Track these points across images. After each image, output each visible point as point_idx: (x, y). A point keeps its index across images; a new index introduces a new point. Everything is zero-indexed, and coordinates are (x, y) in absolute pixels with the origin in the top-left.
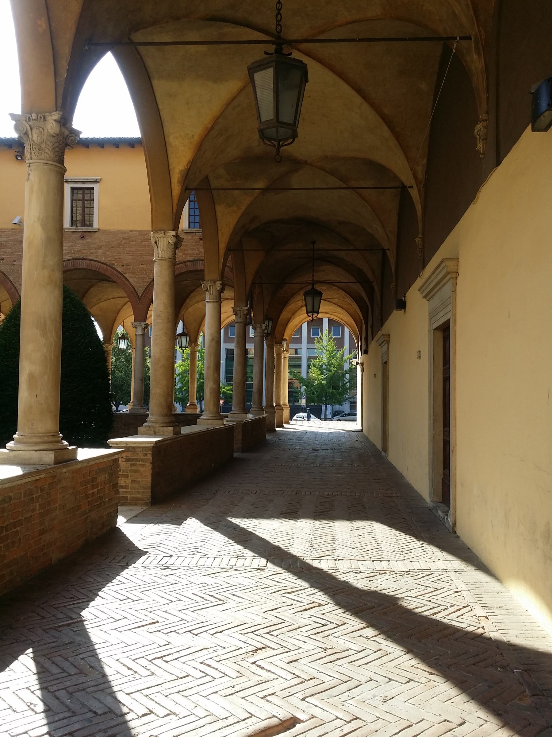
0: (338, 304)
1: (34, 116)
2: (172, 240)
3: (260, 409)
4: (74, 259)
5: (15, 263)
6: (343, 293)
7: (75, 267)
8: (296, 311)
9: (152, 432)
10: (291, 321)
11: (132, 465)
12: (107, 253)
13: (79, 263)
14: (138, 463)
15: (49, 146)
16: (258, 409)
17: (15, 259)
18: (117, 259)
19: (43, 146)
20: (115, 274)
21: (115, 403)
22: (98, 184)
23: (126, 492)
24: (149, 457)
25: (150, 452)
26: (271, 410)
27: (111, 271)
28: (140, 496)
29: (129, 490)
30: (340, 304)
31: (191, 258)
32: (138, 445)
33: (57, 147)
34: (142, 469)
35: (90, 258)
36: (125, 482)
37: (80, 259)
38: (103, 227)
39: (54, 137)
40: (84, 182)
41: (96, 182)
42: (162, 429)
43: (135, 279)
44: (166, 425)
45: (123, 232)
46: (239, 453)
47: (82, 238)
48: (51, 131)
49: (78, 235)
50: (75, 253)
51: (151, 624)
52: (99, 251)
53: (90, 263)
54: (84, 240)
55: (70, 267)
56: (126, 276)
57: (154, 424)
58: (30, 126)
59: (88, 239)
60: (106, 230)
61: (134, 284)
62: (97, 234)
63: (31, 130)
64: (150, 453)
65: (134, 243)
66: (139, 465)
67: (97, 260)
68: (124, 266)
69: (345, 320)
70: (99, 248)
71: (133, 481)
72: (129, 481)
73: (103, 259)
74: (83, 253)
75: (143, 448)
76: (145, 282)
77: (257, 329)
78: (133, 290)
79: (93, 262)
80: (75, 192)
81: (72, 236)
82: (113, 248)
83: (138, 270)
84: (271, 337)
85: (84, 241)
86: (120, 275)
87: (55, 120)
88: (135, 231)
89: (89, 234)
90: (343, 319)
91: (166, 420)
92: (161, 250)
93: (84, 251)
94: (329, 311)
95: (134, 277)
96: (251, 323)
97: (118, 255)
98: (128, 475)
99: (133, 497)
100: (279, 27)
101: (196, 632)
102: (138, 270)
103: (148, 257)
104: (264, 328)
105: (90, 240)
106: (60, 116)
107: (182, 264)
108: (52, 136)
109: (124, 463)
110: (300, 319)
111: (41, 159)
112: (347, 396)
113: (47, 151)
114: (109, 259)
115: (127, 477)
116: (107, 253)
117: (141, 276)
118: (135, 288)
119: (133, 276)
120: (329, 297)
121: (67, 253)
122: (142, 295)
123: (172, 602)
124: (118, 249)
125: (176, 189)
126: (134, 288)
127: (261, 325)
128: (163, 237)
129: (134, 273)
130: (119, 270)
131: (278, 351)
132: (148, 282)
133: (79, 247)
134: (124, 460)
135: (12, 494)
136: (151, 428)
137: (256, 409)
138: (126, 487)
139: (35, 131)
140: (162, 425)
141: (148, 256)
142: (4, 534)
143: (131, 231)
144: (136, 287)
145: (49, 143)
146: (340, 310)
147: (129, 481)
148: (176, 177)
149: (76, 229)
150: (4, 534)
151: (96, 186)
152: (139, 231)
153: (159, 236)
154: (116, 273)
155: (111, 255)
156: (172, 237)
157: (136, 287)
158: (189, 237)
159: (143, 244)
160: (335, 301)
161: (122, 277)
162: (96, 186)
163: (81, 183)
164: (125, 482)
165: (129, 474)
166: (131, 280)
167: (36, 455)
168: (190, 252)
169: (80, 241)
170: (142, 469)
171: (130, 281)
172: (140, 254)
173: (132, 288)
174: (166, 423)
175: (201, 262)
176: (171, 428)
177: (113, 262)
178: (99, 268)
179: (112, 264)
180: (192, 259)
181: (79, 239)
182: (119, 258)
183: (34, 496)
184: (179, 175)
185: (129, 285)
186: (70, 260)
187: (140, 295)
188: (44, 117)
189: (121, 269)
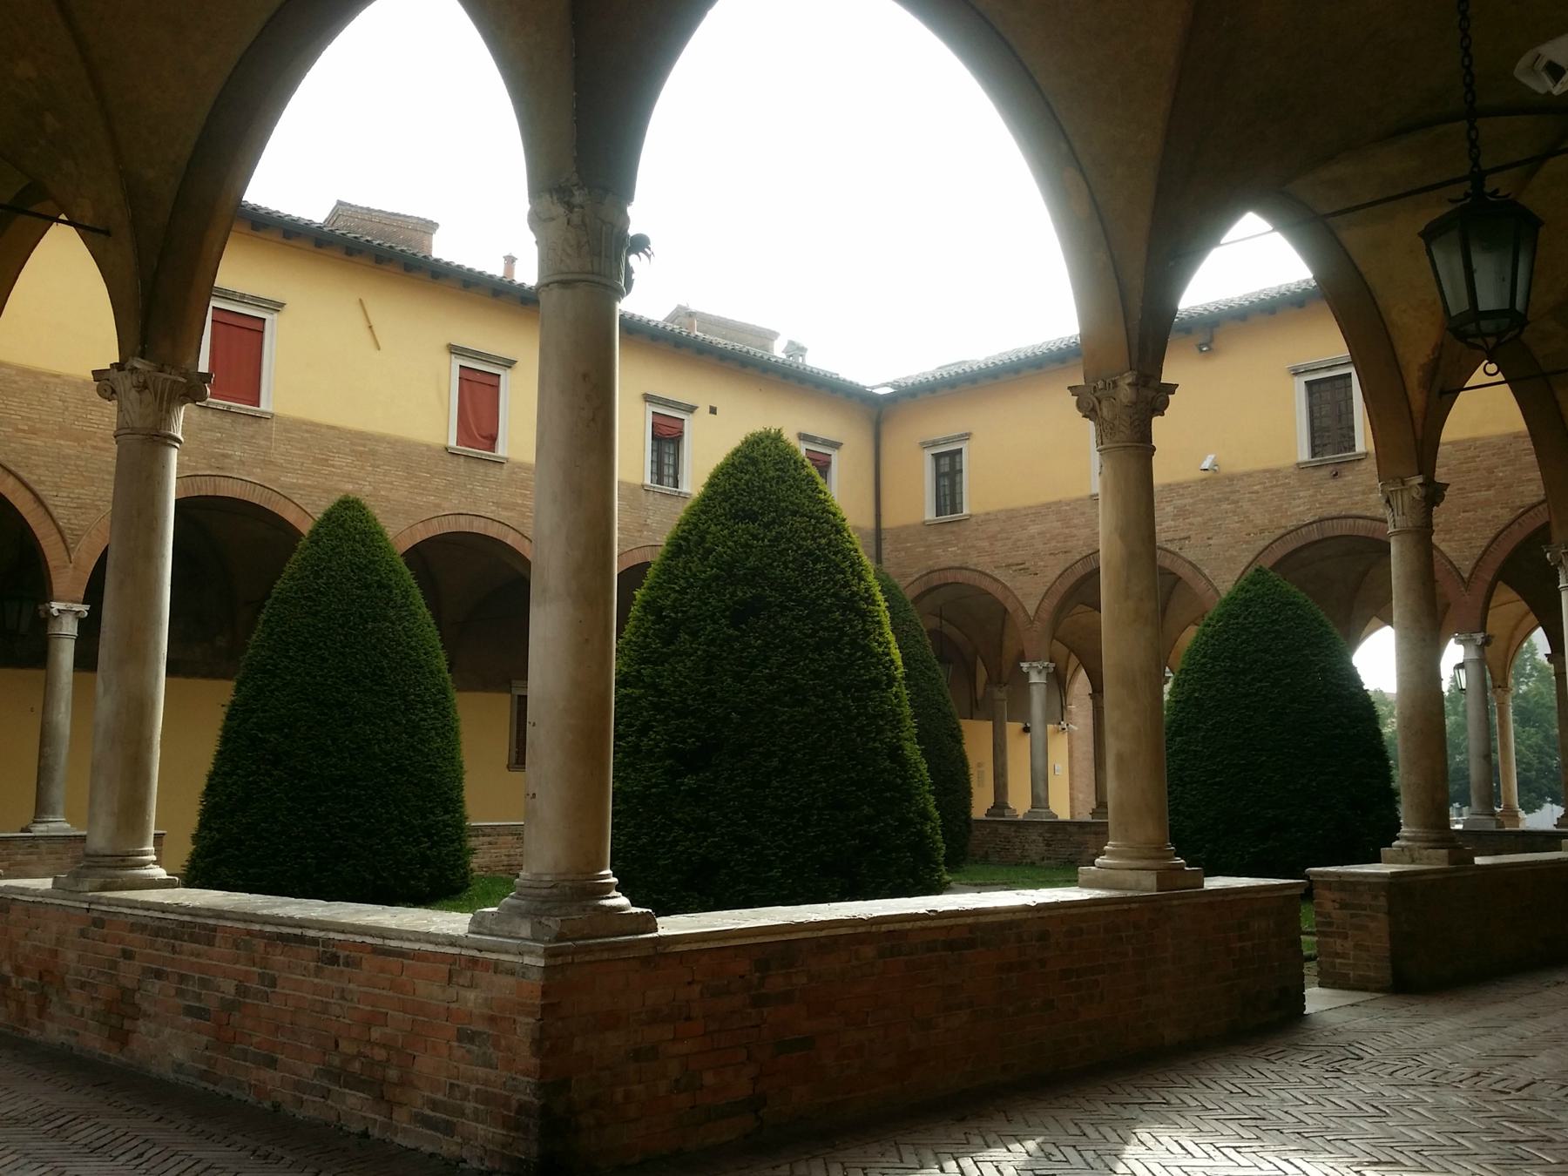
1: (1100, 384)
2: (1417, 493)
4: (1321, 520)
5: (1211, 542)
7: (1325, 536)
9: (1407, 858)
11: (1352, 916)
13: (1333, 526)
14: (1363, 912)
15: (1124, 420)
17: (1210, 535)
19: (1117, 422)
23: (1346, 964)
24: (1382, 901)
25: (1383, 893)
28: (1372, 974)
29: (1351, 962)
32: (1361, 879)
33: (1137, 419)
34: (1372, 925)
35: (1354, 512)
36: (1342, 946)
37: (1332, 519)
39: (1131, 407)
40: (1329, 368)
42: (1425, 853)
43: (1453, 544)
44: (1431, 845)
47: (1335, 475)
48: (1125, 401)
49: (1325, 472)
50: (1321, 508)
51: (1250, 1119)
52: (1371, 496)
55: (1316, 536)
57: (1410, 843)
58: (1097, 398)
59: (1345, 476)
61: (1452, 555)
63: (1100, 403)
64: (1384, 896)
66: (1367, 916)
67: (1368, 514)
71: (1357, 946)
72: (1349, 944)
74: (1340, 505)
75: (1369, 883)
76: (1475, 547)
78: (1449, 567)
79: (1361, 521)
80: (1315, 388)
81: (1316, 474)
83: (1458, 523)
85: (1339, 482)
87: (1129, 384)
89: (1349, 466)
91: (1433, 836)
92: (1400, 513)
95: (1449, 541)
98: (1347, 934)
99: (1360, 975)
100: (1475, 150)
101: (1306, 1135)
102: (1458, 523)
103: (1477, 494)
105: (1351, 478)
106: (1135, 377)
108: (1127, 406)
109: (1338, 911)
111: (1118, 442)
113: (1122, 428)
115: (1346, 937)
117: (1466, 535)
118: (1455, 563)
119: (1448, 537)
121: (1308, 509)
122: (1471, 575)
123: (1307, 1104)
125: (1417, 398)
126: (1451, 563)
128: (1401, 490)
129: (1449, 531)
132: (1481, 546)
133: (1330, 494)
134: (1337, 906)
135: (1084, 925)
136: (1405, 849)
138: (1343, 956)
139: (1104, 403)
140: (1426, 844)
141: (1477, 491)
142: (1074, 980)
145: (1124, 417)
147: (1349, 944)
148: (1414, 377)
149: (1321, 461)
150: (1074, 980)
153: (1393, 489)
156: (1418, 487)
164: (1342, 946)
165: (1350, 932)
167: (1131, 877)
169: (1332, 483)
170: (1372, 925)
171: (1442, 548)
172: (1459, 489)
173: (1447, 564)
174: (1434, 841)
176: (1444, 852)
181: (1326, 479)
183: (1124, 935)
184: (1421, 374)
186: (1314, 522)
188: (1114, 382)
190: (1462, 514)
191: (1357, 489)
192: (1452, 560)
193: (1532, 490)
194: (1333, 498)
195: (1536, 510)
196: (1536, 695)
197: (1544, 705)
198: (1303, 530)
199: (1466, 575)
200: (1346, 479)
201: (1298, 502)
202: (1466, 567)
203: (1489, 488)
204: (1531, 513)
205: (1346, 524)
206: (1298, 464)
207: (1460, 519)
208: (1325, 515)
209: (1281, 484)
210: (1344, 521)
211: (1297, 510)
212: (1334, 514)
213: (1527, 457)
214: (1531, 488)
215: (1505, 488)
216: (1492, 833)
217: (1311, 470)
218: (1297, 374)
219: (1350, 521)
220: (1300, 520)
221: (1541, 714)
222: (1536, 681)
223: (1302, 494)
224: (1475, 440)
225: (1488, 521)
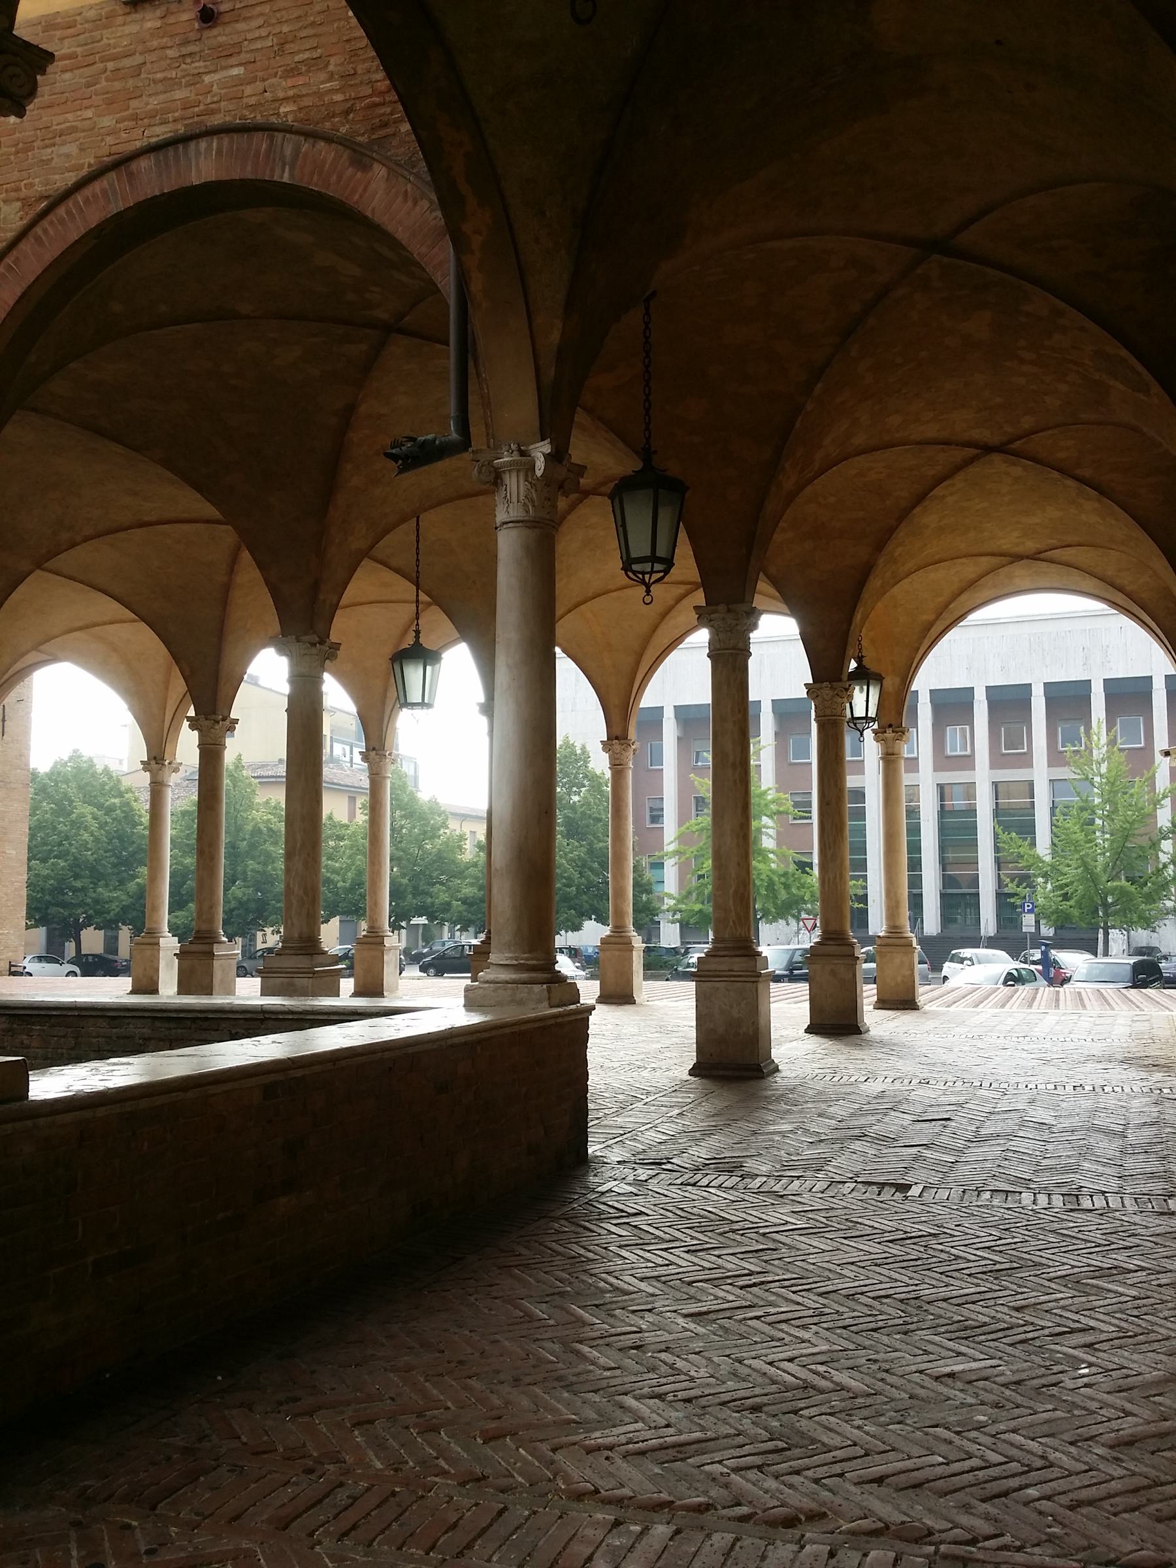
0: (1078, 472)
3: (524, 976)
8: (891, 531)
10: (874, 583)
16: (514, 976)
30: (1086, 472)
31: (159, 130)
69: (1129, 588)
84: (729, 611)
90: (1118, 582)
94: (1054, 542)
96: (465, 443)
107: (113, 175)
110: (940, 599)
120: (1027, 422)
127: (523, 453)
131: (828, 712)
137: (504, 975)
158: (149, 25)
168: (154, 102)
175: (203, 144)
180: (161, 132)
193: (68, 156)
195: (70, 203)
196: (583, 805)
197: (590, 816)
204: (61, 211)
213: (67, 76)
214: (65, 149)
215: (17, 152)
221: (588, 826)
222: (588, 791)
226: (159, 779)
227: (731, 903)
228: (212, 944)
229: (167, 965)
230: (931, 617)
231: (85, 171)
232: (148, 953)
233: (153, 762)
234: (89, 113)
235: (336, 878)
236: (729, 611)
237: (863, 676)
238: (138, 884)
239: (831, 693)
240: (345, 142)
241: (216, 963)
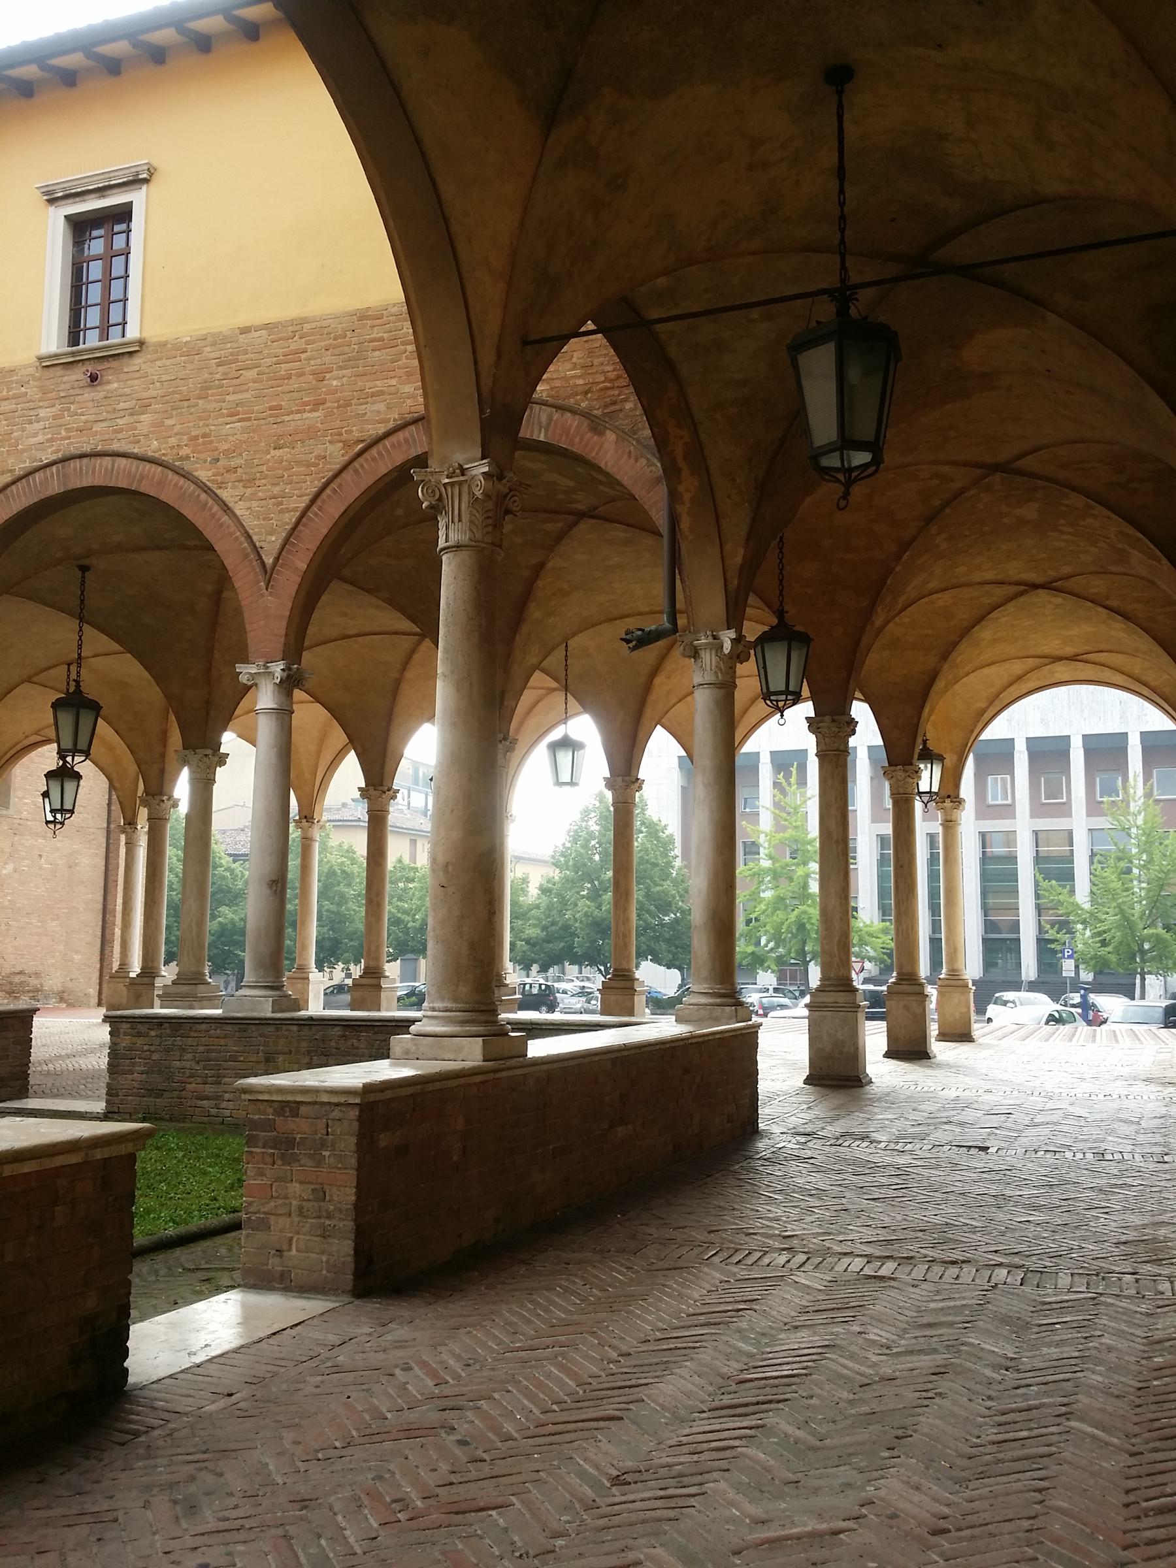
0: (1107, 602)
3: (718, 1000)
6: (1115, 526)
8: (955, 644)
10: (940, 684)
12: (169, 422)
16: (711, 1001)
18: (196, 438)
20: (190, 495)
21: (602, 968)
22: (144, 187)
26: (841, 998)
27: (176, 485)
30: (1115, 603)
35: (115, 447)
37: (82, 456)
38: (155, 332)
40: (101, 191)
41: (135, 182)
43: (254, 504)
45: (218, 340)
46: (314, 1306)
49: (78, 375)
50: (69, 438)
52: (142, 418)
53: (113, 465)
54: (99, 388)
56: (224, 494)
60: (165, 344)
61: (250, 523)
62: (137, 361)
65: (251, 374)
67: (136, 451)
68: (218, 460)
70: (145, 407)
73: (152, 447)
76: (288, 510)
77: (702, 653)
79: (122, 462)
81: (65, 379)
82: (186, 404)
84: (833, 721)
85: (98, 393)
86: (203, 496)
88: (258, 328)
89: (114, 364)
90: (1144, 678)
93: (97, 427)
94: (1089, 648)
97: (201, 424)
102: (265, 468)
103: (298, 416)
104: (727, 647)
105: (115, 385)
107: (413, 428)
110: (992, 690)
112: (769, 878)
114: (173, 441)
116: (169, 422)
117: (276, 490)
118: (255, 538)
119: (249, 491)
120: (1066, 570)
121: (48, 441)
122: (277, 559)
124: (200, 402)
126: (249, 537)
127: (715, 637)
129: (250, 482)
130: (203, 475)
131: (901, 791)
132: (297, 508)
137: (704, 1000)
141: (298, 412)
143: (245, 331)
144: (256, 534)
146: (1121, 635)
151: (137, 198)
152: (265, 326)
154: (194, 491)
155: (177, 429)
157: (256, 534)
159: (283, 373)
160: (1094, 590)
161: (211, 502)
162: (137, 198)
163: (93, 196)
166: (240, 509)
169: (89, 395)
171: (238, 513)
173: (243, 539)
177: (185, 451)
178: (142, 478)
179: (181, 459)
182: (205, 435)
185: (233, 528)
187: (271, 561)
189: (210, 473)
190: (272, 451)
191: (122, 405)
192: (251, 531)
193: (378, 412)
194: (87, 422)
195: (380, 446)
196: (641, 850)
197: (647, 861)
198: (37, 475)
199: (269, 561)
200: (108, 387)
201: (36, 426)
202: (270, 544)
203: (317, 404)
204: (374, 452)
205: (101, 464)
206: (40, 359)
207: (269, 460)
208: (73, 450)
209: (15, 397)
210: (98, 461)
211: (33, 441)
212: (87, 448)
213: (377, 353)
214: (376, 407)
215: (338, 407)
216: (263, 1022)
217: (59, 371)
218: (52, 201)
219: (107, 461)
220: (35, 460)
221: (645, 871)
222: (646, 837)
223: (43, 413)
224: (303, 321)
225: (309, 465)
226: (309, 835)
227: (836, 950)
228: (380, 978)
229: (315, 997)
230: (984, 705)
231: (391, 425)
232: (299, 986)
233: (304, 821)
234: (393, 382)
235: (407, 918)
236: (833, 721)
237: (928, 756)
238: (220, 923)
239: (904, 775)
240: (585, 414)
241: (383, 994)
